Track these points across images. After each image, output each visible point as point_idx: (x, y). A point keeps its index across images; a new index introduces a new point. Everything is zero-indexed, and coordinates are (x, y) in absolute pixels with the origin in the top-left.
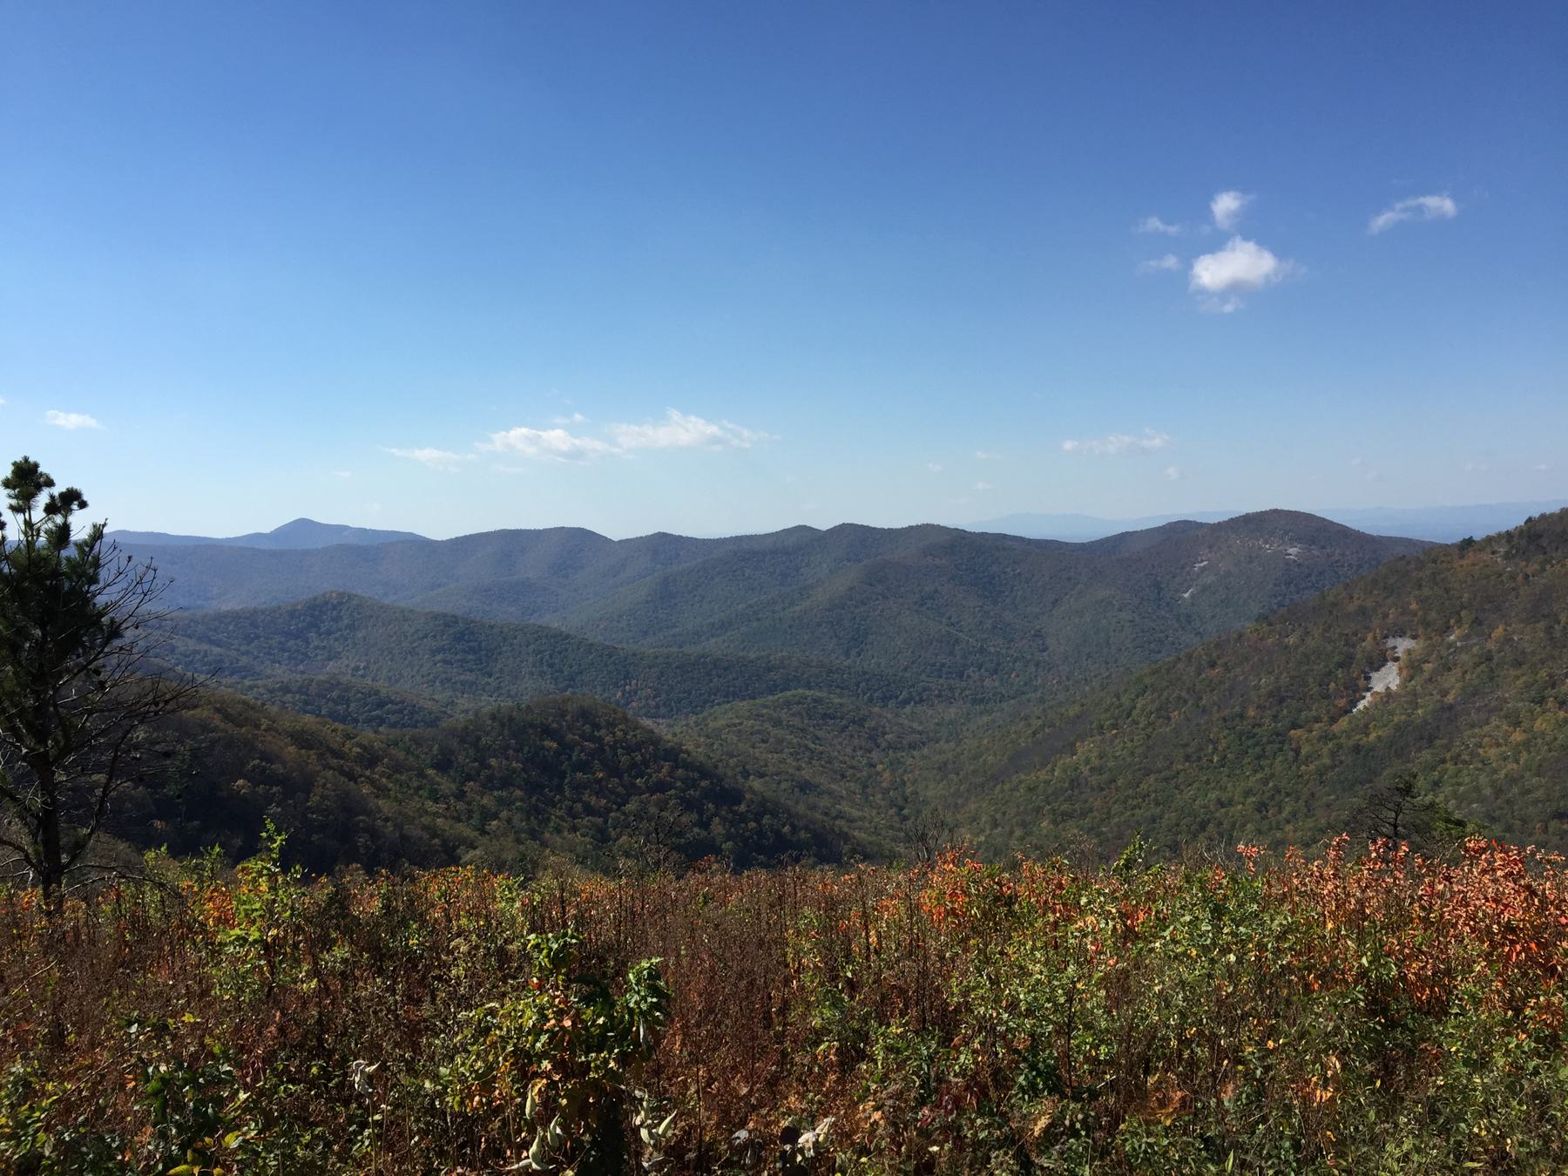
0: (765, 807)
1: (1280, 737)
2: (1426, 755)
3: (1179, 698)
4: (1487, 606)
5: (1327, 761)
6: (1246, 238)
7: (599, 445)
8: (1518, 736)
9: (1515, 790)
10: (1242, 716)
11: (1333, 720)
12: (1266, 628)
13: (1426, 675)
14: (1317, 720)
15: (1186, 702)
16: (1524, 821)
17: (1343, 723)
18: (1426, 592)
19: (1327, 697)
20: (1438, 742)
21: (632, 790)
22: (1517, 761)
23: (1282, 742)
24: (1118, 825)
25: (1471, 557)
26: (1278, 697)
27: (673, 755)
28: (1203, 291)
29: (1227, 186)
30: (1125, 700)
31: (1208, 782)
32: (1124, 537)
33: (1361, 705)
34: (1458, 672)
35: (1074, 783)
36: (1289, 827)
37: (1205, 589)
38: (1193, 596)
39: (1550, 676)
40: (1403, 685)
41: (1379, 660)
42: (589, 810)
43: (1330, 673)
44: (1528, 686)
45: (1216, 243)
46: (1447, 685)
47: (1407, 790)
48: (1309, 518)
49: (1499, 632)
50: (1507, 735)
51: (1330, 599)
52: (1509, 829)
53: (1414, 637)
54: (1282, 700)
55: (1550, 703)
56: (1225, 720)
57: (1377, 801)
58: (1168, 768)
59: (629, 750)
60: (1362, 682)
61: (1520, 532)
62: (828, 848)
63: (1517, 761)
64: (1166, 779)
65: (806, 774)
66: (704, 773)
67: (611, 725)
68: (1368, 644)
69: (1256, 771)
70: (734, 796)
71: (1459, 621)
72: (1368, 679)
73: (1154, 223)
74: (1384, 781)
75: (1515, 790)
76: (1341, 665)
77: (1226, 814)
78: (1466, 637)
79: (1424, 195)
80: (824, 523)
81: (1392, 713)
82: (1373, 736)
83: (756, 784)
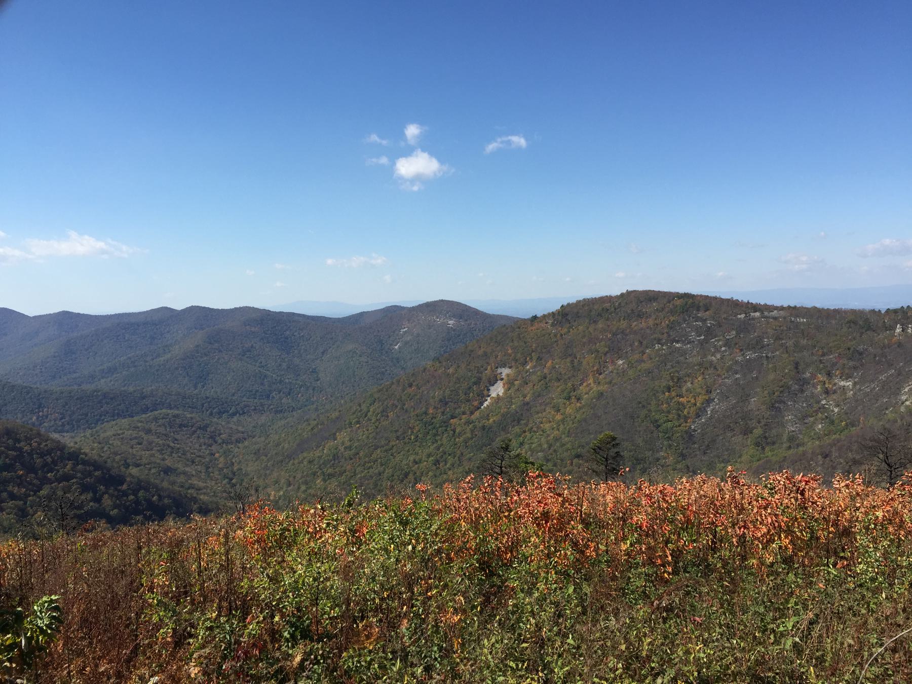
0: (141, 485)
1: (446, 423)
2: (517, 429)
3: (393, 405)
4: (544, 351)
5: (469, 435)
6: (423, 150)
7: (17, 253)
8: (559, 417)
9: (558, 444)
10: (426, 413)
11: (472, 413)
12: (438, 364)
13: (516, 387)
14: (464, 413)
15: (397, 407)
16: (562, 460)
17: (477, 414)
18: (516, 343)
19: (468, 401)
20: (522, 422)
21: (45, 481)
22: (558, 430)
23: (447, 426)
24: (361, 479)
25: (536, 325)
26: (444, 402)
27: (75, 456)
28: (401, 178)
29: (413, 121)
30: (364, 407)
31: (408, 451)
32: (362, 314)
33: (485, 404)
34: (530, 385)
35: (335, 457)
36: (450, 473)
37: (406, 343)
38: (400, 348)
39: (573, 385)
40: (505, 393)
41: (493, 381)
42: (13, 497)
43: (470, 388)
44: (563, 391)
45: (408, 152)
46: (526, 392)
47: (506, 449)
48: (459, 304)
49: (549, 364)
50: (554, 416)
51: (470, 348)
52: (555, 465)
53: (510, 367)
54: (446, 404)
55: (573, 400)
56: (417, 416)
57: (493, 455)
58: (387, 444)
59: (42, 455)
60: (485, 392)
61: (558, 312)
62: (182, 508)
63: (558, 430)
64: (386, 451)
65: (168, 462)
66: (97, 466)
67: (28, 439)
68: (488, 372)
69: (433, 443)
70: (120, 480)
71: (531, 359)
72: (489, 390)
73: (374, 138)
74: (498, 443)
75: (558, 444)
76: (475, 383)
77: (418, 468)
78: (535, 367)
80: (179, 306)
81: (500, 408)
82: (491, 420)
83: (134, 471)
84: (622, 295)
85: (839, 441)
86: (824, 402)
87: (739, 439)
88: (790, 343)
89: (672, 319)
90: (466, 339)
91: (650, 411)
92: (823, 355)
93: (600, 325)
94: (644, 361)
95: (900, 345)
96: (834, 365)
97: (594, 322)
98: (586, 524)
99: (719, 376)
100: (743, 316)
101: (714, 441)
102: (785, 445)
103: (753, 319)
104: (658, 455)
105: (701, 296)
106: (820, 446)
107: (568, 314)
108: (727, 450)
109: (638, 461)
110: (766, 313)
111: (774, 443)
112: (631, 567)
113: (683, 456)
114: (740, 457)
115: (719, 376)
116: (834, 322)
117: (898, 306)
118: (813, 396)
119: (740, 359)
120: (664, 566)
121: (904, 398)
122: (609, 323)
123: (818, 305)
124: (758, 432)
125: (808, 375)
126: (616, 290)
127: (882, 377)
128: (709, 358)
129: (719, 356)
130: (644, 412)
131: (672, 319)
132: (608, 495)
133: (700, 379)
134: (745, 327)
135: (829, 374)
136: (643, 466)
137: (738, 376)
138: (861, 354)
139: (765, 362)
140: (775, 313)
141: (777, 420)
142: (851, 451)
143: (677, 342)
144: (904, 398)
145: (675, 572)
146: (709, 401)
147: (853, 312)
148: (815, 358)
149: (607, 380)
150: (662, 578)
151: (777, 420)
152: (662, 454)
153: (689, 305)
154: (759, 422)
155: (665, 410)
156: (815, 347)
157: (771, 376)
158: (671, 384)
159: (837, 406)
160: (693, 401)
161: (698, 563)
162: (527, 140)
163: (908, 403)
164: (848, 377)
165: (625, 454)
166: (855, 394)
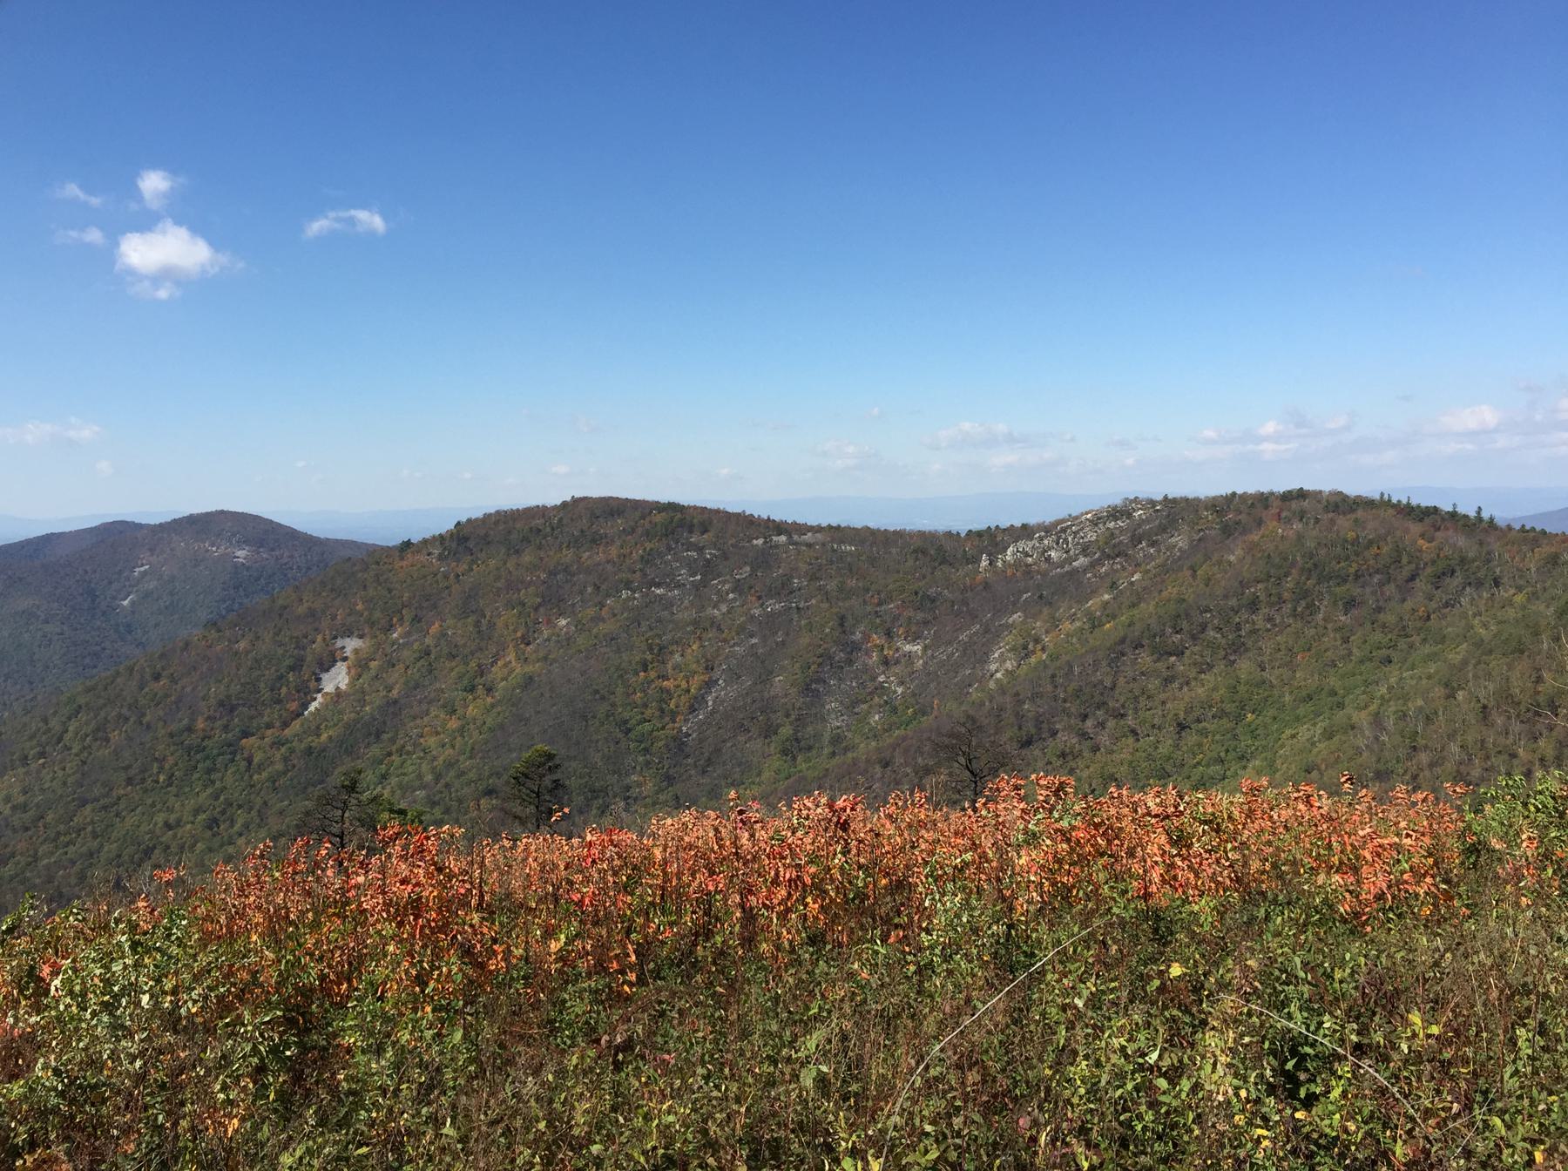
1: (232, 748)
2: (375, 751)
3: (120, 716)
4: (425, 604)
5: (279, 767)
6: (179, 222)
8: (453, 724)
9: (452, 773)
10: (190, 729)
11: (286, 725)
12: (214, 634)
13: (373, 673)
14: (269, 726)
15: (127, 719)
16: (460, 801)
17: (296, 725)
18: (371, 592)
19: (279, 701)
20: (385, 736)
22: (453, 747)
23: (234, 753)
24: (48, 867)
25: (410, 558)
26: (228, 706)
28: (131, 272)
29: (154, 166)
30: (55, 724)
31: (153, 805)
33: (313, 707)
34: (401, 667)
36: (241, 841)
37: (147, 595)
38: (133, 603)
39: (479, 666)
40: (351, 684)
41: (327, 663)
43: (281, 677)
44: (460, 678)
45: (146, 222)
46: (391, 681)
47: (352, 788)
48: (256, 519)
49: (435, 629)
50: (444, 726)
51: (280, 602)
52: (447, 811)
53: (361, 637)
54: (232, 709)
55: (480, 690)
56: (171, 735)
57: (326, 801)
58: (107, 795)
60: (312, 684)
61: (451, 534)
63: (453, 747)
64: (105, 808)
68: (318, 646)
69: (206, 787)
71: (401, 619)
72: (319, 680)
73: (73, 190)
74: (337, 778)
75: (452, 773)
76: (292, 668)
77: (175, 836)
78: (408, 634)
79: (355, 207)
81: (341, 712)
82: (324, 737)
84: (564, 504)
85: (904, 739)
86: (882, 678)
87: (756, 745)
88: (832, 585)
89: (648, 546)
90: (276, 584)
91: (613, 705)
92: (880, 604)
93: (527, 558)
94: (603, 620)
95: (987, 586)
96: (896, 618)
97: (517, 552)
98: (489, 912)
99: (725, 641)
100: (760, 541)
101: (718, 751)
102: (826, 751)
103: (777, 546)
104: (627, 781)
105: (695, 508)
106: (878, 749)
107: (469, 539)
108: (740, 764)
109: (595, 793)
110: (796, 537)
111: (810, 748)
112: (567, 982)
113: (670, 779)
114: (759, 775)
115: (725, 641)
116: (894, 551)
117: (983, 527)
118: (866, 669)
119: (757, 612)
120: (623, 972)
121: (993, 667)
122: (542, 554)
123: (872, 525)
124: (786, 731)
125: (858, 636)
126: (553, 495)
127: (963, 637)
128: (710, 611)
129: (724, 608)
130: (603, 708)
131: (648, 546)
132: (538, 853)
133: (695, 647)
134: (764, 560)
135: (889, 634)
136: (599, 801)
137: (754, 641)
138: (933, 601)
139: (796, 617)
140: (808, 537)
141: (814, 711)
142: (922, 754)
143: (658, 585)
144: (993, 667)
145: (641, 981)
146: (709, 685)
147: (921, 534)
148: (869, 608)
149: (541, 655)
150: (619, 994)
151: (814, 711)
152: (634, 778)
153: (676, 524)
154: (788, 716)
155: (639, 702)
156: (868, 590)
157: (805, 640)
158: (649, 657)
159: (902, 683)
160: (684, 685)
161: (684, 959)
162: (385, 218)
163: (999, 675)
164: (915, 638)
165: (572, 783)
166: (926, 663)
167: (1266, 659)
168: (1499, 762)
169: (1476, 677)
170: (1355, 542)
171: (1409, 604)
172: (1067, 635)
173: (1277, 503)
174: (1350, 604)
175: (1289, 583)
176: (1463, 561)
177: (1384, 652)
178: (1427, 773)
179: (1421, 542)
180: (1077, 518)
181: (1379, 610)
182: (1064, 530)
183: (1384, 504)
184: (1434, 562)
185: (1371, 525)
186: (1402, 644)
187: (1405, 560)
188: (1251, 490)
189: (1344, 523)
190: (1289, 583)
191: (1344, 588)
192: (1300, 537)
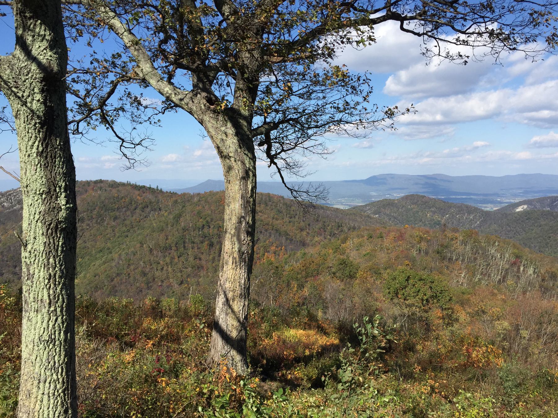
167: (87, 239)
168: (154, 266)
169: (149, 240)
170: (118, 197)
171: (134, 218)
172: (11, 236)
173: (93, 184)
174: (116, 218)
175: (95, 212)
176: (150, 203)
177: (126, 234)
178: (133, 272)
179: (138, 197)
180: (15, 190)
181: (125, 220)
182: (10, 195)
183: (129, 184)
184: (142, 203)
185: (123, 192)
186: (131, 231)
187: (133, 203)
188: (84, 180)
189: (114, 191)
190: (95, 212)
191: (114, 213)
192: (100, 196)
